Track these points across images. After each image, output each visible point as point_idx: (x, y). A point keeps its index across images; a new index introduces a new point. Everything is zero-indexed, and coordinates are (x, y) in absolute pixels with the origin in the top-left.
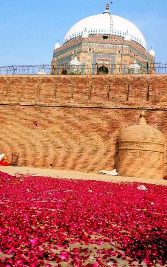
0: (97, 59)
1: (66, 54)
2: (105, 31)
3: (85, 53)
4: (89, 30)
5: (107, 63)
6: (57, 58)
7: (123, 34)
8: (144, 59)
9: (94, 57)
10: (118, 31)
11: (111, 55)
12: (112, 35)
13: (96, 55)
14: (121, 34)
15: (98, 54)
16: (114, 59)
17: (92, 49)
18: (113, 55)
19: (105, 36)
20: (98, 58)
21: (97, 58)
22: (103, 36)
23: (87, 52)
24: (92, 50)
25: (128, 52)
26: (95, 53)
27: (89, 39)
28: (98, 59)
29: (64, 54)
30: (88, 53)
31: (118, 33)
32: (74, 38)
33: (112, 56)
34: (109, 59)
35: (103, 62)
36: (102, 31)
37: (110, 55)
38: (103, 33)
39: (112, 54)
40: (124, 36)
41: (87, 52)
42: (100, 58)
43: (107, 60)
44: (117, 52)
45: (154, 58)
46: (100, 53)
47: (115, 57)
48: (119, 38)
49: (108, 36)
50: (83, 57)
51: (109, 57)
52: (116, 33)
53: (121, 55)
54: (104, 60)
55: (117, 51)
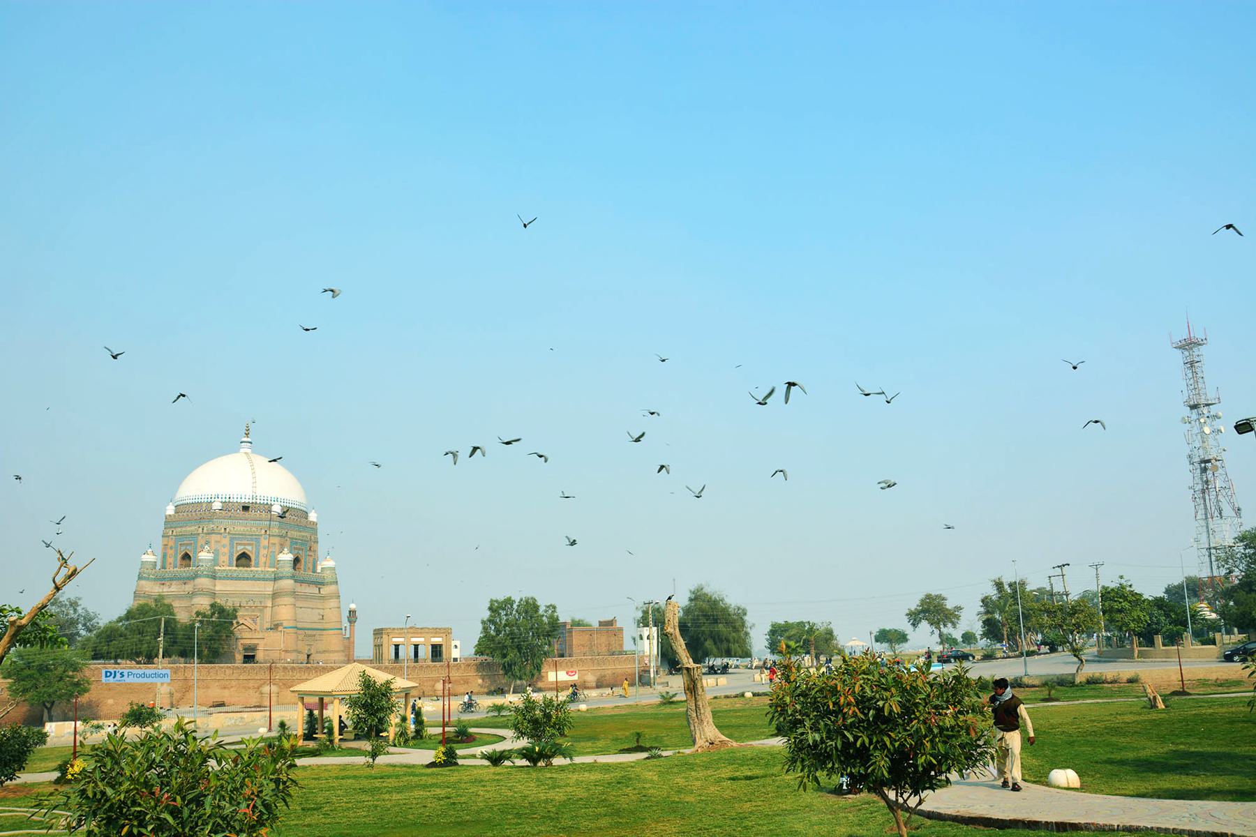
5: (249, 548)
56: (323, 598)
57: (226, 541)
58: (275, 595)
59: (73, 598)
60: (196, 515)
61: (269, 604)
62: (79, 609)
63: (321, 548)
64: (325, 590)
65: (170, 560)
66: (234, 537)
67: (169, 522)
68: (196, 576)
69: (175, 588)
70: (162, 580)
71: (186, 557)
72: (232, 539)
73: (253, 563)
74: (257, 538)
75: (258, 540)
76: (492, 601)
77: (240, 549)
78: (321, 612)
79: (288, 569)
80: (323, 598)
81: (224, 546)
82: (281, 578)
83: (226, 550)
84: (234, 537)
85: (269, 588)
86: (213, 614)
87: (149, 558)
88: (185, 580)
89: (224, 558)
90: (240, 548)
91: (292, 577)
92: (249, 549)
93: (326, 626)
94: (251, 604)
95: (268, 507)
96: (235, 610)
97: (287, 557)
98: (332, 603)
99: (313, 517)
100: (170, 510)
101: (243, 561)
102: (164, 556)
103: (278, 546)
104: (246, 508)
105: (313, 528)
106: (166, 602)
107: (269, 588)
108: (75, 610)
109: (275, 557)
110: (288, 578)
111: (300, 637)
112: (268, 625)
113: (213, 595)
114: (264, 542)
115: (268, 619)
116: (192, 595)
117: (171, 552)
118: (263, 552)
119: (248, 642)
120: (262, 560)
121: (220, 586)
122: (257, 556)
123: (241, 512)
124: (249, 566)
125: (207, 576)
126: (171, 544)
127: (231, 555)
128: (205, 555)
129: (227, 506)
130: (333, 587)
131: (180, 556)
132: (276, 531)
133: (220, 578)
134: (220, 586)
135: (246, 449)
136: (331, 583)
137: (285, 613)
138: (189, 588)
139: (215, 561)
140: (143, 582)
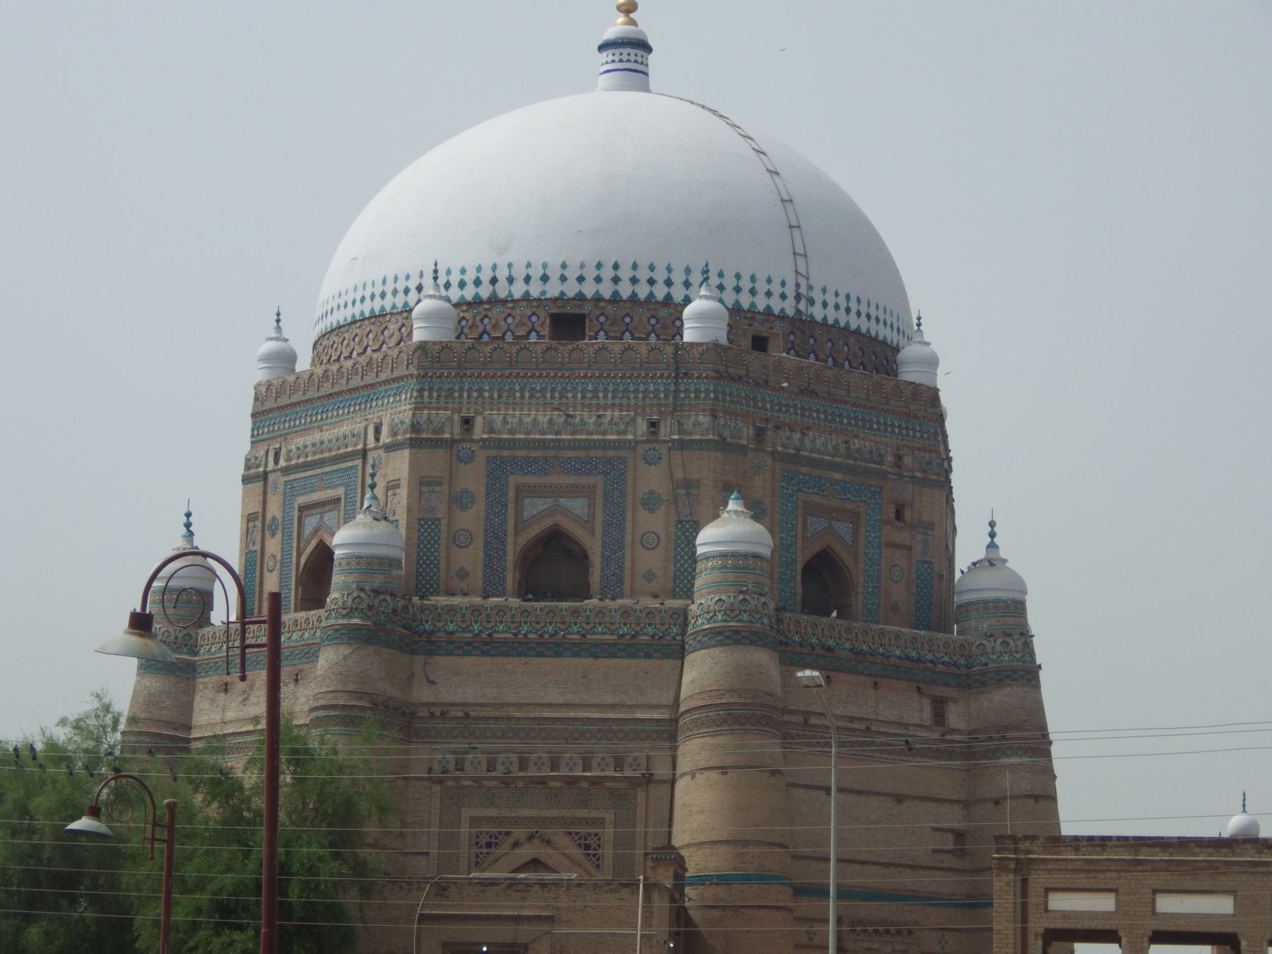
3: (440, 452)
5: (578, 506)
11: (600, 453)
15: (520, 453)
17: (479, 423)
18: (611, 453)
19: (569, 309)
21: (513, 480)
22: (555, 311)
24: (479, 432)
26: (500, 444)
31: (651, 282)
34: (589, 480)
35: (550, 501)
37: (592, 453)
38: (553, 290)
39: (605, 445)
43: (574, 491)
44: (642, 426)
46: (528, 444)
49: (587, 309)
54: (558, 491)
72: (497, 470)
83: (471, 519)
89: (471, 558)
90: (535, 506)
92: (577, 513)
114: (652, 479)
124: (584, 593)
127: (494, 538)
132: (700, 423)
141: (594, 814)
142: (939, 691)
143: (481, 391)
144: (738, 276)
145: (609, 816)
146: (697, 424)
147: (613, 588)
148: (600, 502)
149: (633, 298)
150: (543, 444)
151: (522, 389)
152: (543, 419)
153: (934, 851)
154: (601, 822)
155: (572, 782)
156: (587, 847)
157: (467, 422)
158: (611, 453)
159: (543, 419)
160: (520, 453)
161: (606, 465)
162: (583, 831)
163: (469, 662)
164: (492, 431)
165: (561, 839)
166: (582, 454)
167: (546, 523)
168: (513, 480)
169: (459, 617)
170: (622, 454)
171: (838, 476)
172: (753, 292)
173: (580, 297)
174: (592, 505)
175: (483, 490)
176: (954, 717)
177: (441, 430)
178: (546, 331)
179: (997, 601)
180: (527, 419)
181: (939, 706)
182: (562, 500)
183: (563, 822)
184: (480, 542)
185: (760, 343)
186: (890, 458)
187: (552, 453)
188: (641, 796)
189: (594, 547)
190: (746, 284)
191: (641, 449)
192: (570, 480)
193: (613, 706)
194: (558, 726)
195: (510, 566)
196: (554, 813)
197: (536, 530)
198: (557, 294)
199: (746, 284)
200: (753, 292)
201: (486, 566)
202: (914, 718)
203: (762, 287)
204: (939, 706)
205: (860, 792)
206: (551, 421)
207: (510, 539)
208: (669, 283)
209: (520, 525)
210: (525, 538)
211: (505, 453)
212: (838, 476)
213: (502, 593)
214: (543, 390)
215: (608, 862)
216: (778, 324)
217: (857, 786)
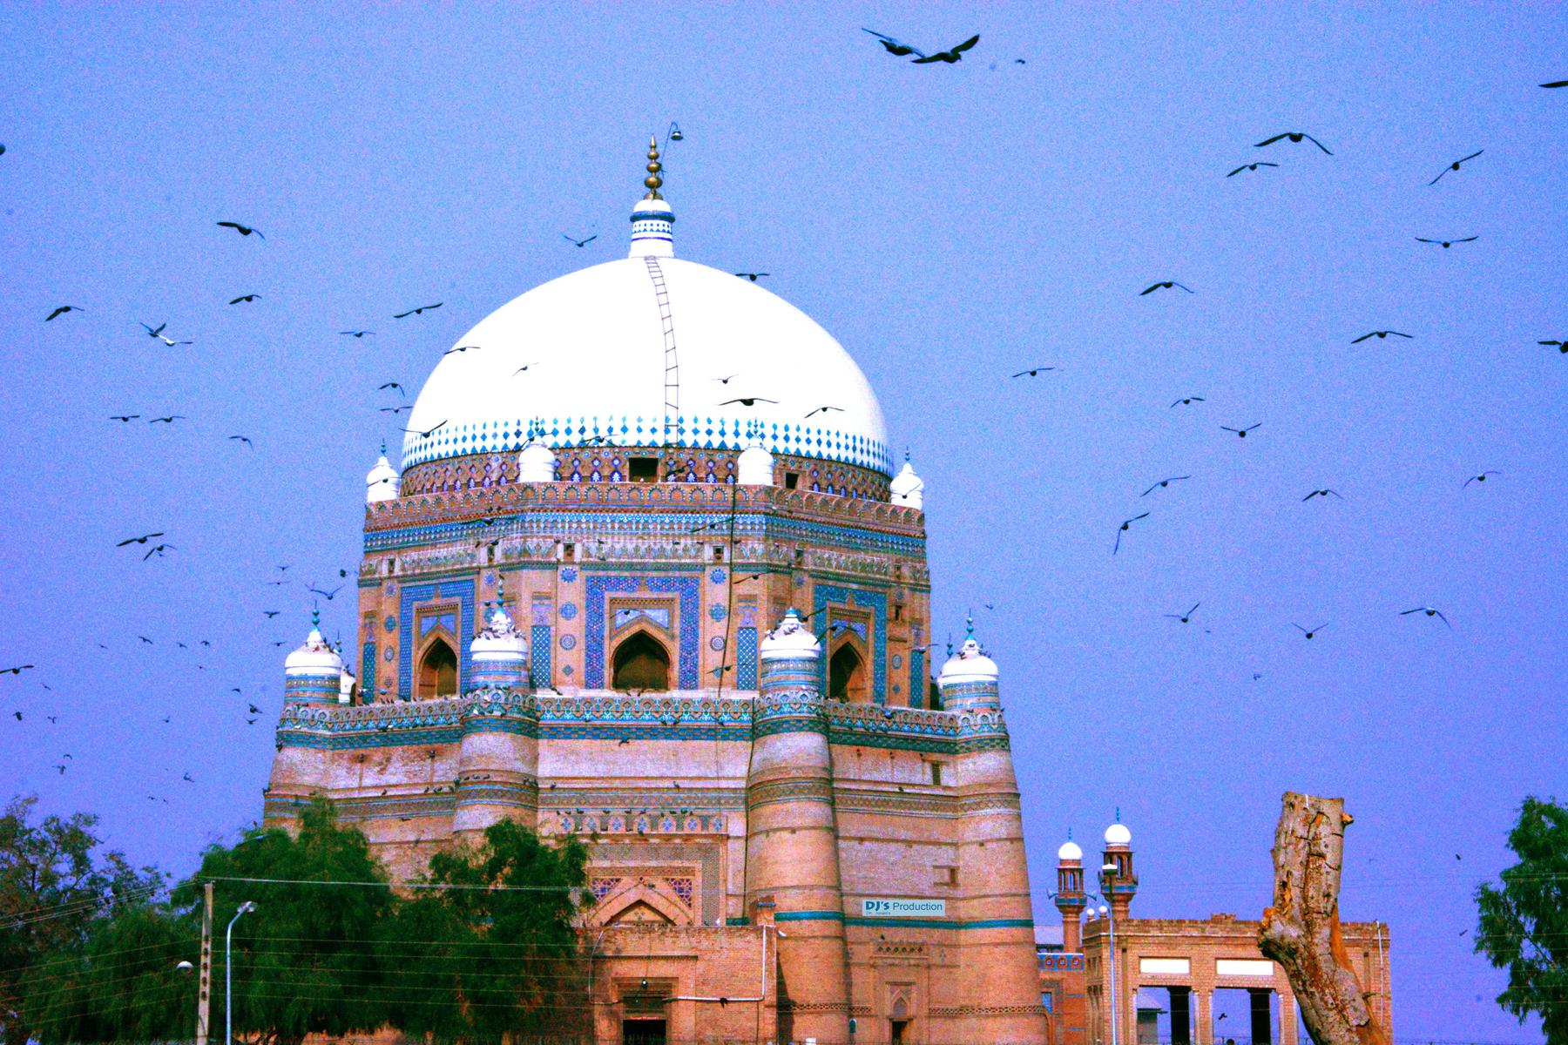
0: (607, 601)
1: (442, 552)
2: (639, 430)
3: (547, 573)
4: (555, 422)
5: (659, 615)
6: (392, 563)
7: (737, 434)
8: (854, 556)
9: (589, 589)
10: (709, 421)
11: (677, 574)
12: (680, 446)
13: (599, 579)
14: (723, 433)
15: (612, 574)
16: (694, 593)
17: (578, 549)
18: (685, 574)
19: (645, 455)
20: (614, 594)
21: (608, 595)
23: (554, 566)
25: (760, 548)
27: (561, 488)
28: (613, 601)
29: (431, 553)
30: (562, 568)
31: (709, 432)
32: (474, 453)
33: (684, 580)
36: (624, 430)
38: (631, 439)
39: (681, 567)
40: (743, 442)
41: (554, 566)
42: (621, 595)
43: (657, 603)
44: (708, 553)
45: (922, 518)
46: (621, 566)
47: (696, 580)
48: (718, 457)
49: (659, 454)
50: (538, 596)
51: (666, 584)
52: (696, 432)
53: (726, 571)
55: (706, 547)
56: (951, 803)
57: (573, 594)
58: (757, 793)
59: (66, 816)
60: (471, 493)
61: (736, 827)
62: (97, 858)
63: (942, 609)
64: (964, 772)
65: (388, 669)
66: (602, 580)
67: (382, 531)
68: (467, 726)
69: (398, 773)
70: (358, 745)
71: (441, 657)
72: (594, 590)
73: (675, 673)
74: (682, 584)
75: (690, 590)
76: (1529, 806)
77: (626, 624)
78: (945, 856)
79: (799, 695)
80: (951, 803)
81: (567, 612)
82: (776, 728)
83: (574, 627)
84: (602, 580)
85: (732, 765)
86: (494, 867)
87: (310, 661)
88: (435, 739)
89: (571, 658)
91: (821, 724)
92: (658, 620)
93: (967, 911)
94: (668, 826)
95: (724, 461)
96: (576, 854)
97: (794, 644)
98: (990, 822)
99: (907, 489)
100: (382, 486)
101: (641, 665)
102: (369, 654)
103: (764, 607)
104: (643, 467)
105: (909, 534)
106: (340, 823)
107: (732, 765)
108: (81, 863)
109: (755, 647)
110: (799, 725)
111: (862, 953)
112: (735, 908)
113: (529, 790)
114: (715, 594)
115: (734, 884)
116: (462, 790)
117: (387, 640)
118: (713, 630)
119: (636, 971)
120: (710, 659)
121: (553, 762)
122: (690, 648)
123: (622, 484)
124: (661, 684)
125: (504, 725)
126: (389, 608)
128: (496, 648)
129: (573, 461)
130: (986, 764)
131: (417, 655)
132: (755, 549)
133: (555, 733)
134: (553, 762)
135: (650, 243)
136: (982, 745)
137: (793, 859)
138: (444, 771)
139: (533, 674)
140: (293, 754)
141: (686, 864)
142: (936, 757)
143: (579, 522)
144: (775, 427)
145: (698, 865)
146: (753, 551)
147: (690, 681)
148: (678, 613)
149: (695, 447)
150: (631, 567)
151: (613, 522)
152: (630, 547)
153: (936, 884)
154: (690, 871)
155: (668, 838)
156: (681, 890)
157: (569, 549)
158: (685, 574)
159: (630, 547)
160: (612, 574)
161: (682, 584)
162: (677, 878)
163: (582, 744)
164: (589, 556)
165: (661, 885)
166: (663, 574)
167: (636, 629)
168: (608, 595)
169: (573, 708)
170: (695, 574)
171: (855, 586)
172: (787, 439)
173: (654, 446)
174: (671, 616)
175: (584, 604)
176: (947, 777)
177: (548, 555)
178: (627, 473)
179: (978, 683)
180: (617, 546)
181: (936, 768)
182: (647, 612)
183: (660, 871)
184: (582, 645)
185: (791, 480)
186: (891, 569)
187: (638, 574)
188: (722, 850)
189: (674, 650)
190: (781, 433)
191: (709, 571)
192: (655, 595)
193: (699, 778)
194: (655, 794)
195: (607, 665)
196: (653, 863)
197: (626, 635)
198: (634, 443)
199: (781, 433)
200: (787, 439)
201: (587, 665)
202: (917, 779)
203: (793, 434)
204: (936, 768)
205: (883, 840)
206: (637, 548)
207: (607, 642)
208: (723, 433)
209: (615, 631)
210: (616, 644)
211: (601, 573)
212: (855, 586)
213: (601, 686)
214: (630, 522)
215: (698, 902)
216: (805, 463)
217: (880, 836)
